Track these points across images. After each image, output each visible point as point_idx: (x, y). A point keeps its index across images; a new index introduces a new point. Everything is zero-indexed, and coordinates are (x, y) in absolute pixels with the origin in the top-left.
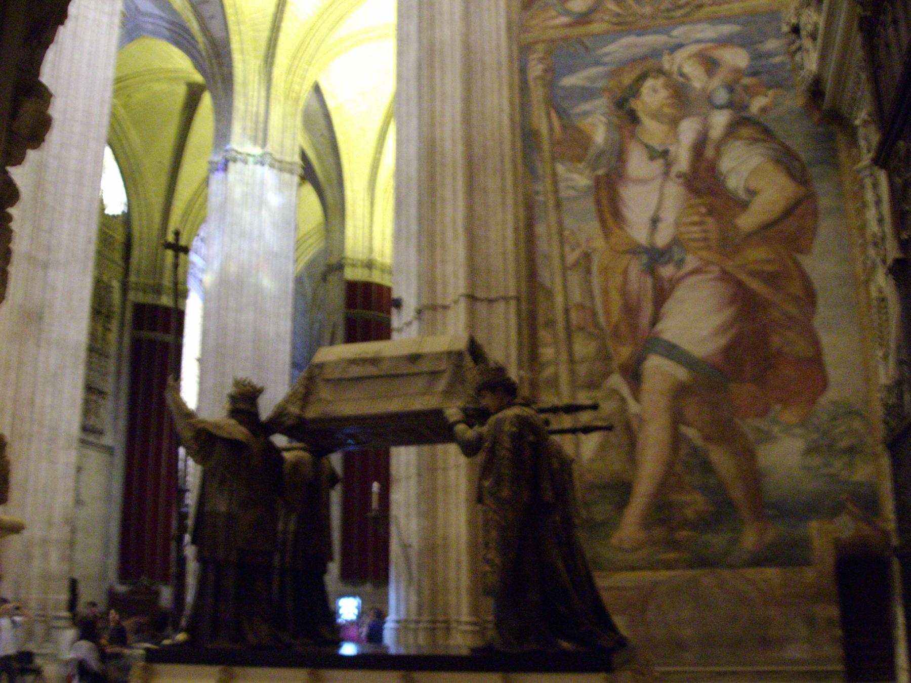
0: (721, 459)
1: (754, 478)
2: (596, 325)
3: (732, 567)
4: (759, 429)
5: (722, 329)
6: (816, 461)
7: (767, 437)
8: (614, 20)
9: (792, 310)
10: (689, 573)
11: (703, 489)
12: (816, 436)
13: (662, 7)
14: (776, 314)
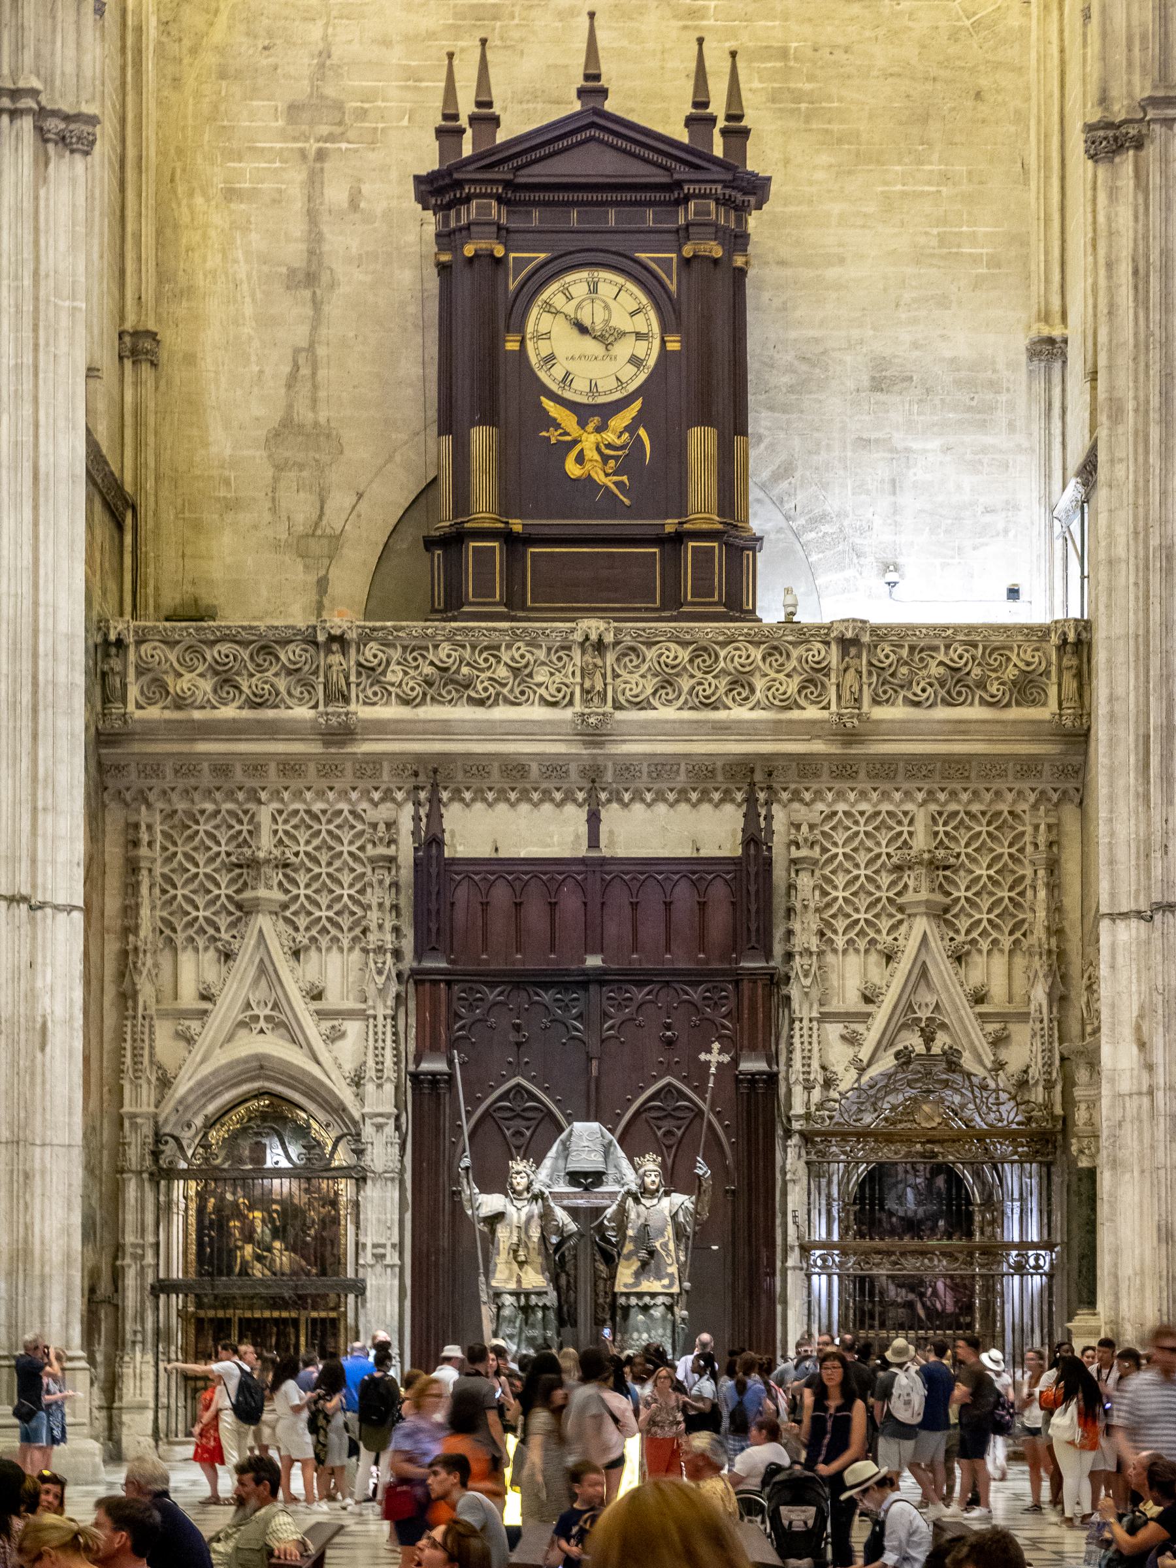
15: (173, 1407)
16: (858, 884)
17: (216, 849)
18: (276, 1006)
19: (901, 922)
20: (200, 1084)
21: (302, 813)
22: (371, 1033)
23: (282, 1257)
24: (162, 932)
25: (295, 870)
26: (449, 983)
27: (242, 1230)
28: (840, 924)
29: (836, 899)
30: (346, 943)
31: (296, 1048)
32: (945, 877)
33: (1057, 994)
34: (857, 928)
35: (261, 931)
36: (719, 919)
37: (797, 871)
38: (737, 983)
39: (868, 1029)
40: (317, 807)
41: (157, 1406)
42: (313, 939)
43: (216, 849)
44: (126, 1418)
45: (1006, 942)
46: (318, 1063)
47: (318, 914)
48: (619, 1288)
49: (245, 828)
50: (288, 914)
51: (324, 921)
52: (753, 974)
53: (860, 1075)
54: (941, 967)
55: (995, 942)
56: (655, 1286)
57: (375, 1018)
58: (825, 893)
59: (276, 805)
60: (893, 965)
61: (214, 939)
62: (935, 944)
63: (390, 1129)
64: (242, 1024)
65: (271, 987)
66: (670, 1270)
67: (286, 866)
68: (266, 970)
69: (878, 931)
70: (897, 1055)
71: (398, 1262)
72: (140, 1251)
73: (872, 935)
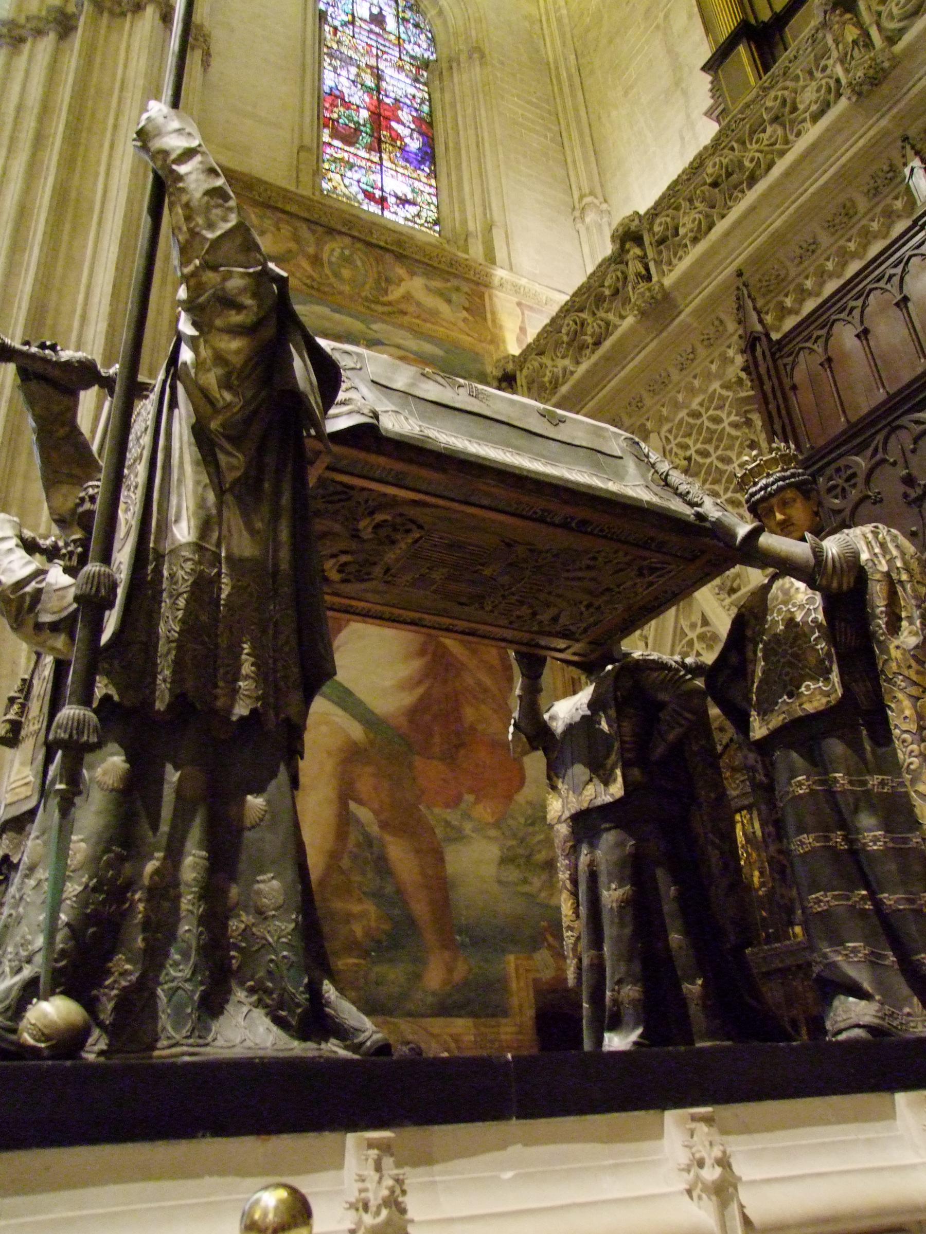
0: (399, 853)
1: (440, 887)
3: (410, 1014)
4: (448, 824)
5: (406, 685)
6: (512, 874)
7: (458, 837)
8: (308, 282)
9: (487, 681)
11: (377, 896)
12: (514, 843)
13: (363, 294)
14: (470, 681)
21: (686, 418)
40: (695, 405)
59: (666, 427)
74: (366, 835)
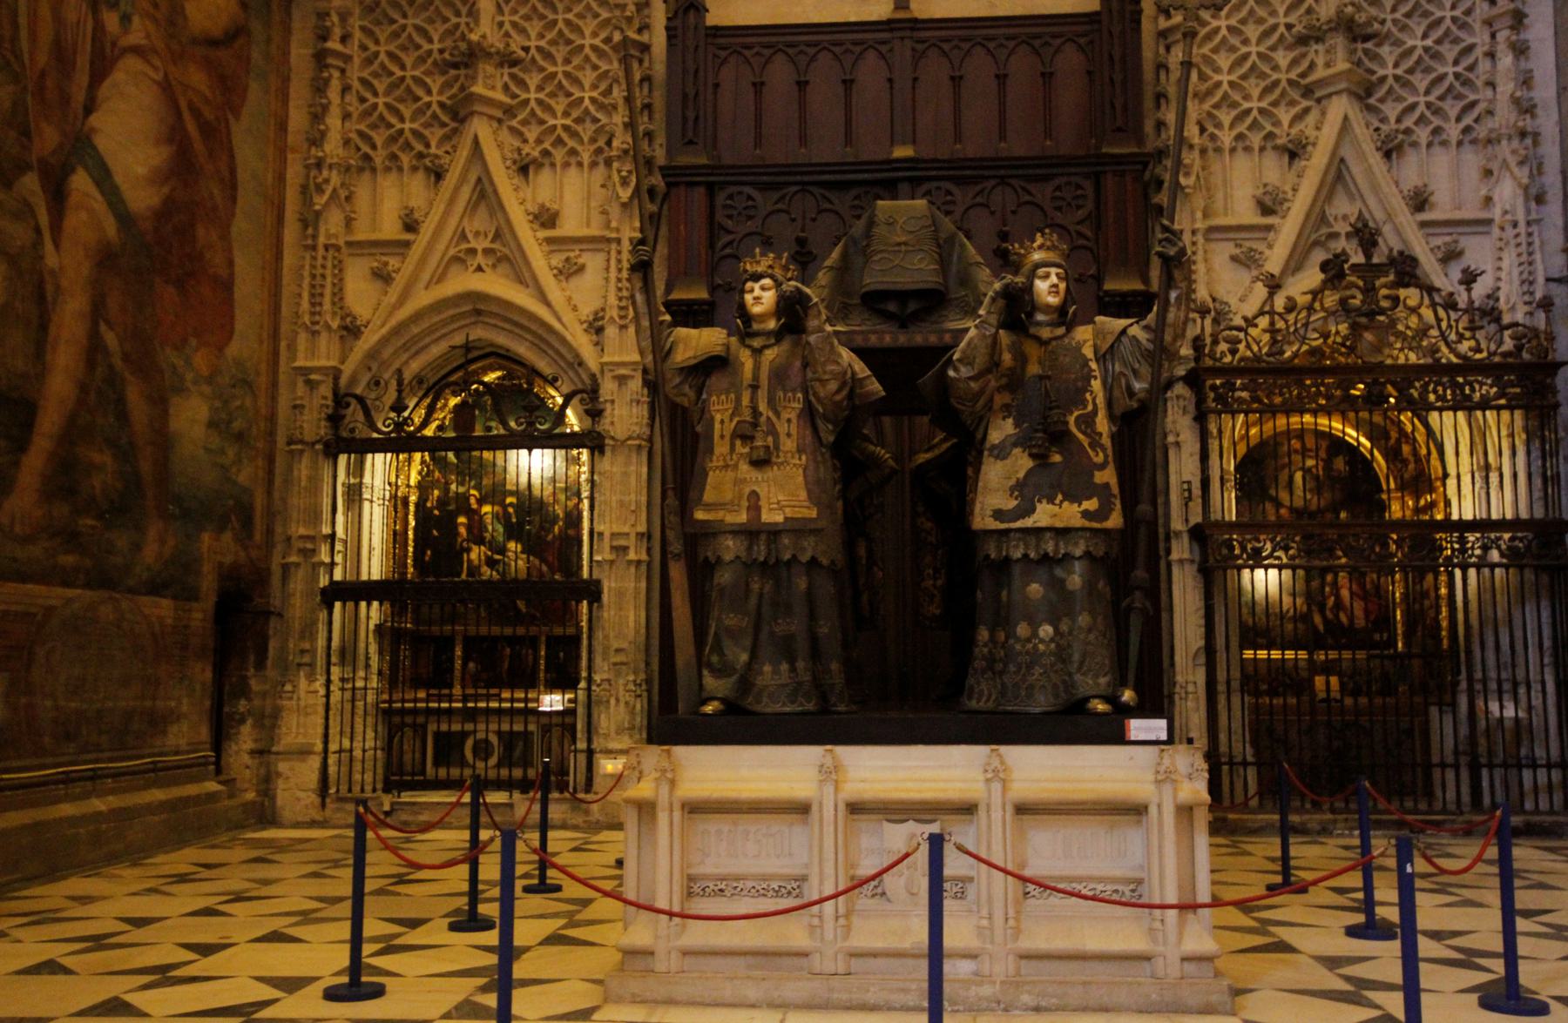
2: (18, 57)
3: (131, 591)
5: (159, 177)
10: (89, 594)
15: (358, 753)
16: (1248, 65)
17: (426, 46)
18: (497, 236)
19: (1307, 111)
20: (397, 331)
22: (613, 262)
23: (517, 559)
24: (359, 149)
25: (525, 70)
26: (711, 188)
27: (469, 528)
28: (1226, 117)
29: (1218, 84)
30: (586, 157)
31: (521, 288)
32: (1366, 52)
33: (1533, 191)
34: (1249, 121)
35: (476, 141)
36: (1070, 97)
37: (1168, 49)
38: (1097, 179)
39: (1270, 247)
41: (326, 750)
42: (546, 153)
43: (426, 46)
44: (283, 767)
45: (1453, 131)
46: (548, 304)
47: (552, 122)
48: (982, 519)
49: (463, 20)
50: (514, 123)
51: (559, 131)
52: (1118, 160)
53: (1271, 295)
54: (1367, 162)
55: (1437, 131)
56: (1069, 513)
57: (619, 241)
58: (1203, 77)
60: (1300, 164)
61: (421, 156)
62: (1360, 130)
63: (636, 384)
64: (457, 259)
65: (492, 215)
66: (1100, 477)
67: (515, 63)
68: (485, 194)
69: (1277, 123)
70: (1324, 267)
71: (644, 557)
72: (309, 546)
73: (1269, 128)
74: (111, 367)
